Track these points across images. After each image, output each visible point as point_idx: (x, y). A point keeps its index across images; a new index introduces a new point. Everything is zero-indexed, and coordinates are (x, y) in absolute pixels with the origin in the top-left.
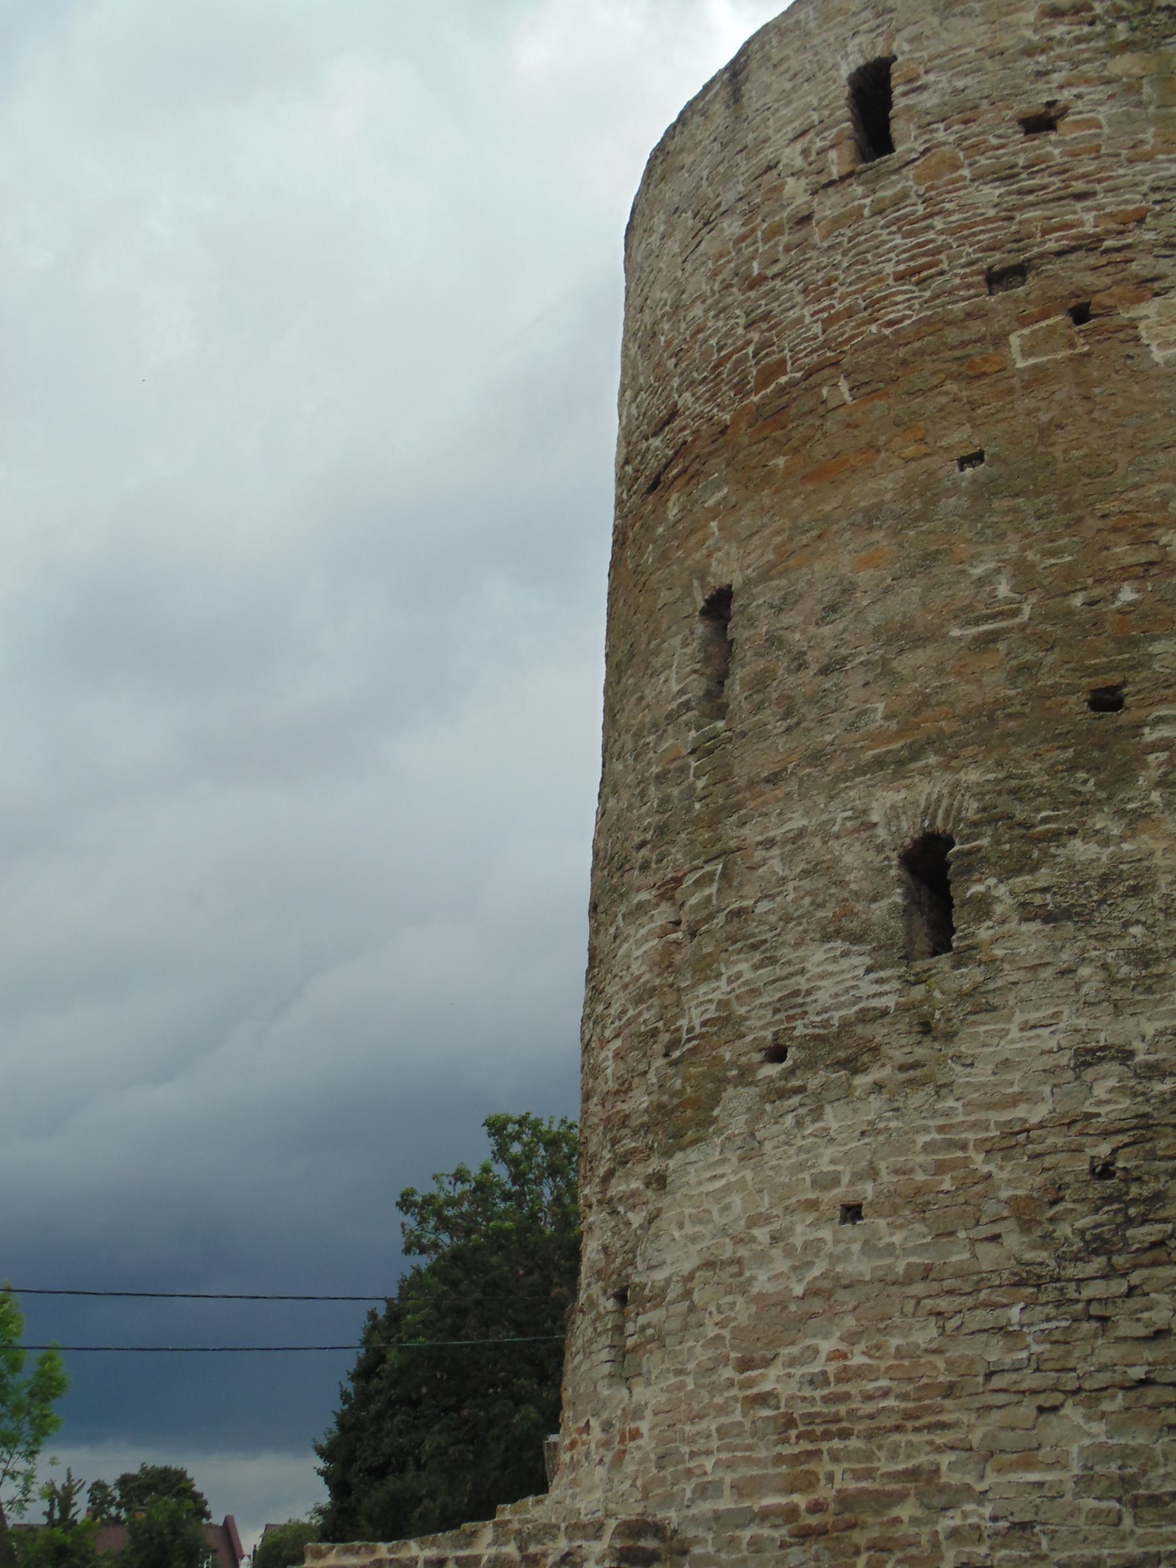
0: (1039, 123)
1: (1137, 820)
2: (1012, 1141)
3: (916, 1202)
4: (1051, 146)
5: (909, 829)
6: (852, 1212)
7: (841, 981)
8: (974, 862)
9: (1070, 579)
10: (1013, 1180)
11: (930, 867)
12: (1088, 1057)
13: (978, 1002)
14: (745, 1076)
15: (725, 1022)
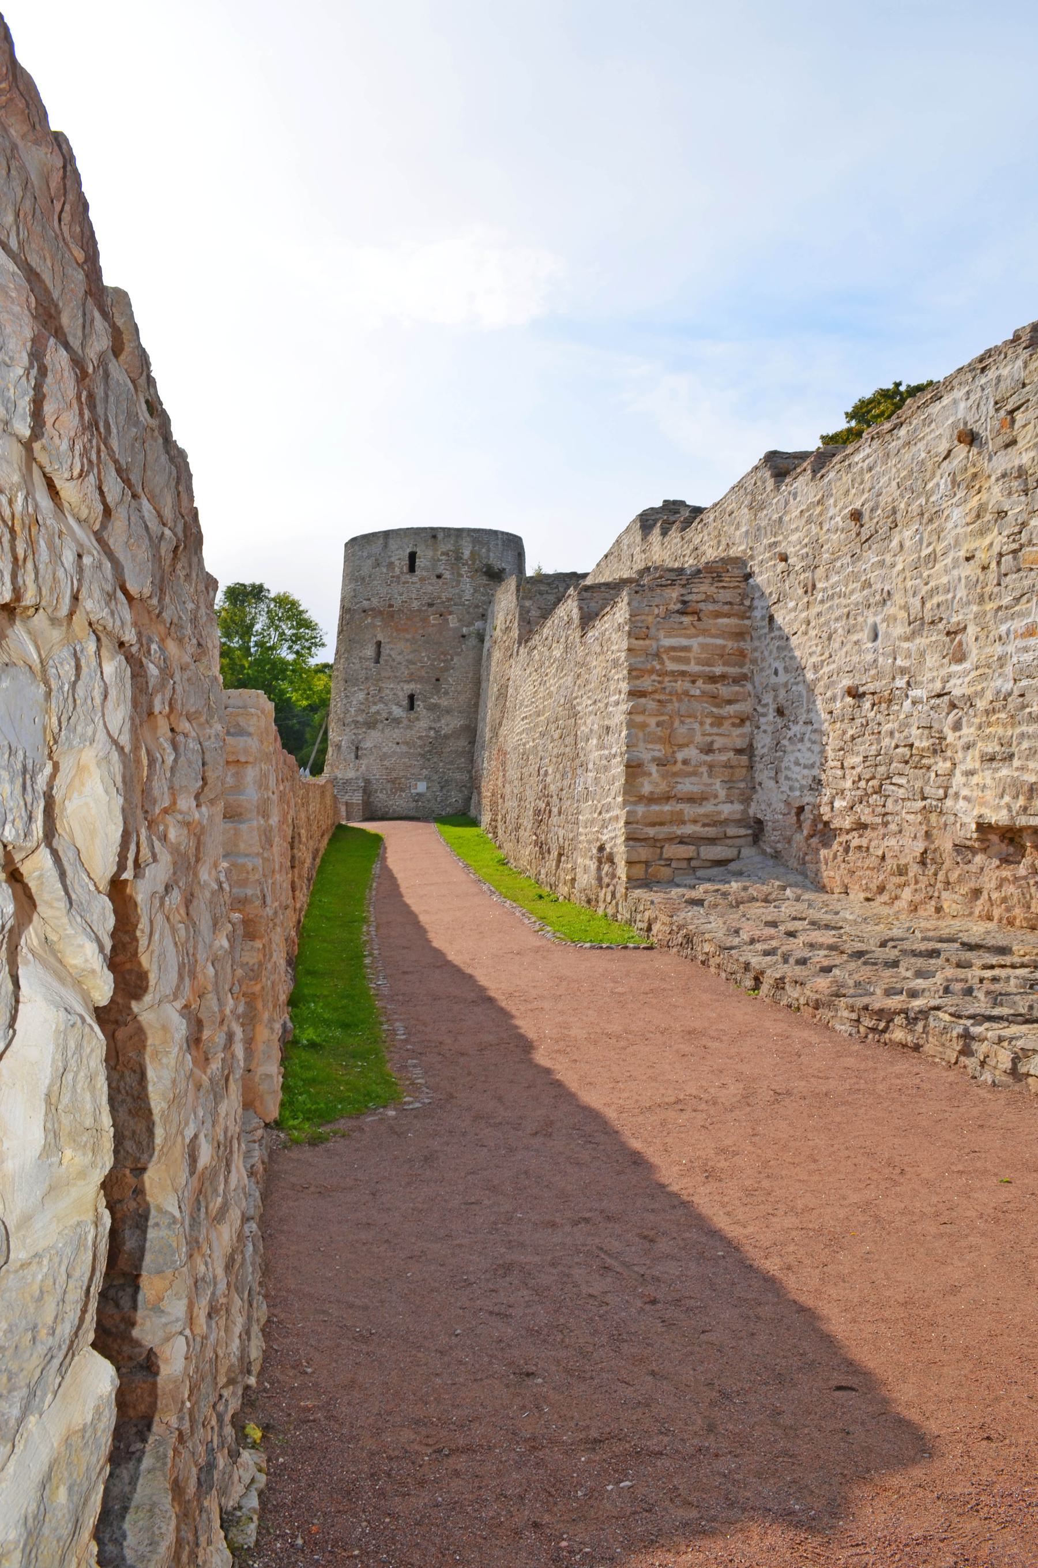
0: (439, 577)
1: (440, 698)
2: (420, 738)
3: (407, 743)
4: (440, 581)
5: (409, 692)
6: (398, 743)
7: (398, 712)
8: (418, 699)
9: (435, 659)
10: (419, 742)
11: (411, 698)
12: (431, 728)
13: (418, 719)
14: (382, 722)
15: (378, 712)
